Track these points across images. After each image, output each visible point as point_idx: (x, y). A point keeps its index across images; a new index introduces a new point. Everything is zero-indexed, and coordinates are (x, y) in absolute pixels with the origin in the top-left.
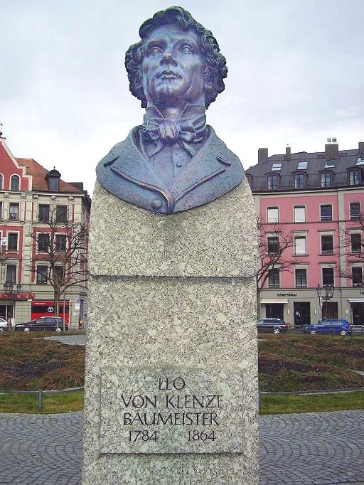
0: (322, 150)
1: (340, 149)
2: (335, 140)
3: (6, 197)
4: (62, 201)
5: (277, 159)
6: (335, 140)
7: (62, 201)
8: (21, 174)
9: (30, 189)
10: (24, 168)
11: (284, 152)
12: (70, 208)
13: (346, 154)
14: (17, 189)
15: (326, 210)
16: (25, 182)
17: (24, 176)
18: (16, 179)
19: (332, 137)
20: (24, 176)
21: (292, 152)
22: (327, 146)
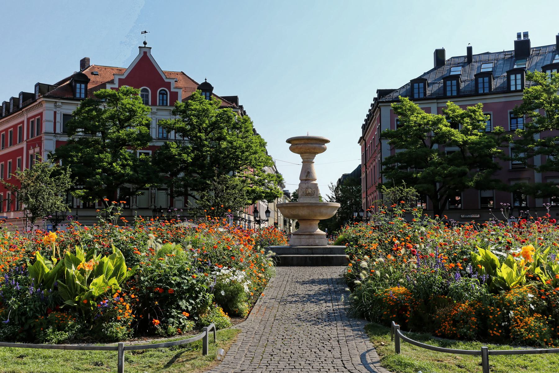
0: (512, 48)
5: (456, 61)
6: (526, 35)
8: (169, 89)
14: (167, 105)
16: (174, 96)
17: (172, 90)
18: (163, 93)
20: (172, 90)
21: (474, 52)
22: (516, 42)
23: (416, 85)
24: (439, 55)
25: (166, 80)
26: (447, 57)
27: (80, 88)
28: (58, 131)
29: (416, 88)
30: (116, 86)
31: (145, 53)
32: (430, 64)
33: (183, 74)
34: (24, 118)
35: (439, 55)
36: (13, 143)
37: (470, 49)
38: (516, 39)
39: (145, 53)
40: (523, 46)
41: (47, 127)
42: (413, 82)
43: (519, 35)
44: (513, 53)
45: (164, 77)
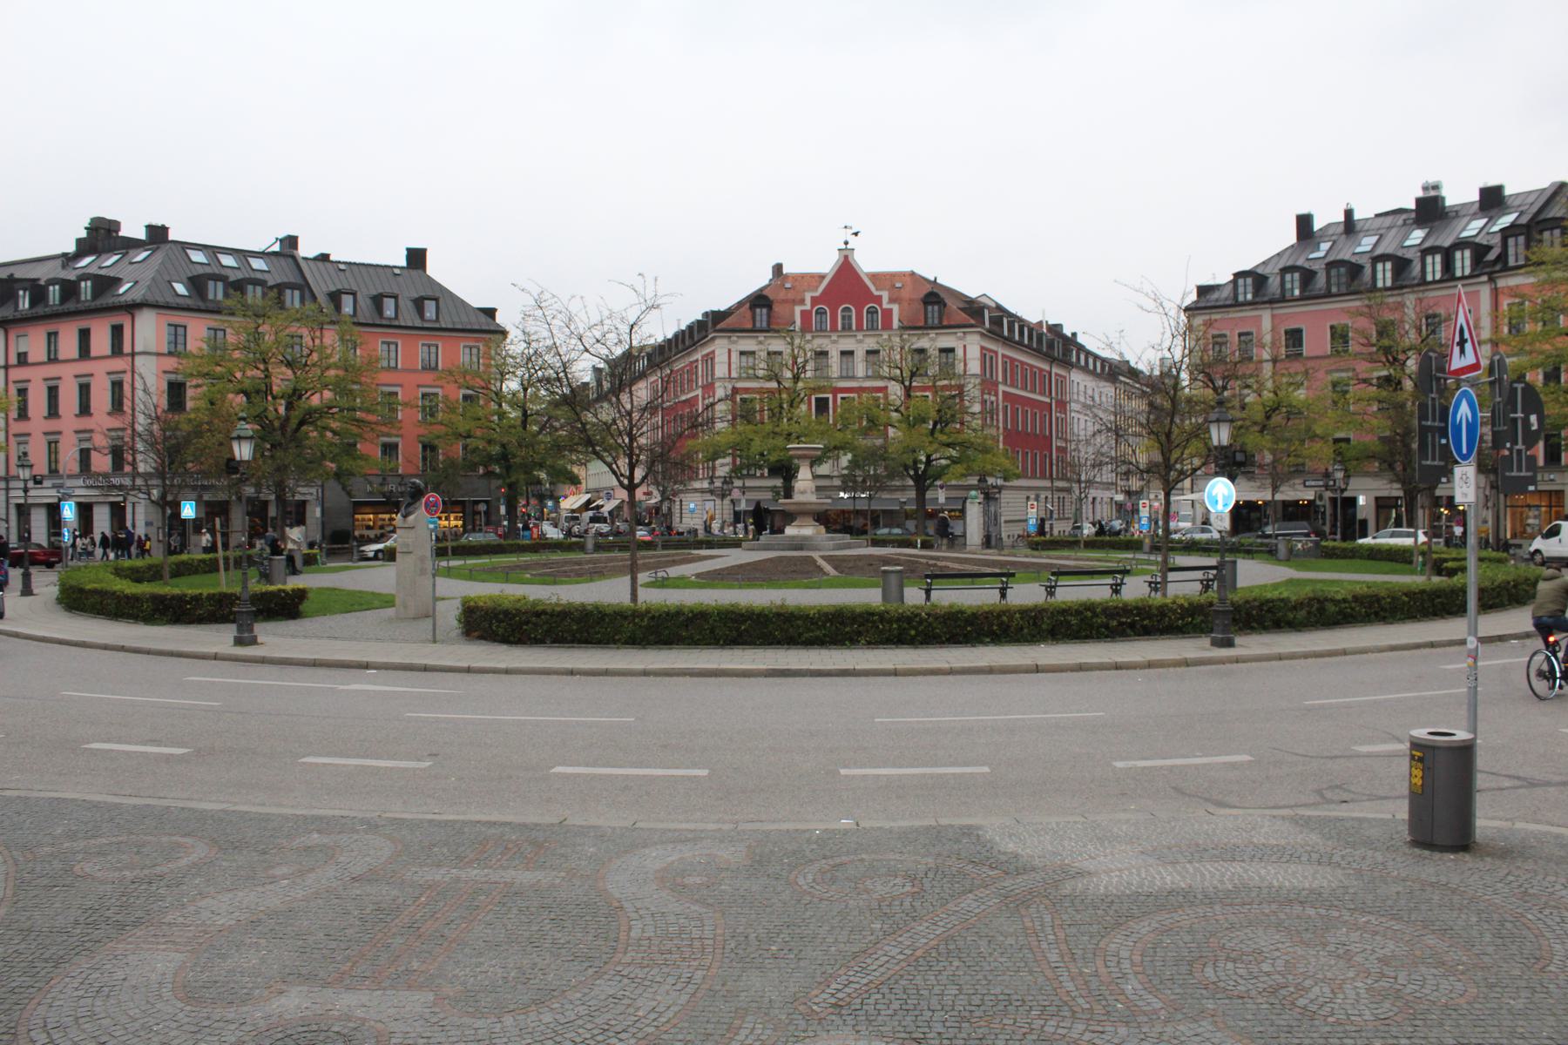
1: (1448, 203)
2: (1436, 187)
3: (860, 342)
4: (946, 341)
7: (946, 341)
9: (896, 324)
10: (885, 295)
11: (1342, 219)
12: (959, 353)
13: (1457, 213)
15: (1295, 337)
17: (886, 305)
19: (1432, 180)
20: (886, 305)
21: (1357, 216)
22: (1419, 201)
23: (1241, 281)
24: (1304, 222)
25: (876, 293)
26: (1317, 226)
27: (761, 313)
28: (734, 375)
29: (1255, 286)
30: (808, 307)
31: (846, 257)
32: (1291, 237)
33: (913, 274)
34: (698, 356)
35: (1304, 222)
36: (691, 390)
37: (1349, 213)
38: (1420, 194)
39: (846, 257)
40: (1430, 209)
41: (721, 370)
42: (1238, 275)
43: (1425, 188)
44: (1413, 215)
45: (872, 288)
